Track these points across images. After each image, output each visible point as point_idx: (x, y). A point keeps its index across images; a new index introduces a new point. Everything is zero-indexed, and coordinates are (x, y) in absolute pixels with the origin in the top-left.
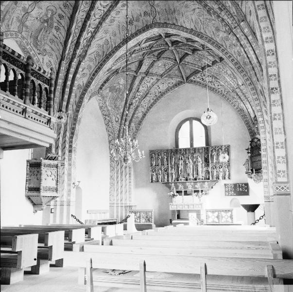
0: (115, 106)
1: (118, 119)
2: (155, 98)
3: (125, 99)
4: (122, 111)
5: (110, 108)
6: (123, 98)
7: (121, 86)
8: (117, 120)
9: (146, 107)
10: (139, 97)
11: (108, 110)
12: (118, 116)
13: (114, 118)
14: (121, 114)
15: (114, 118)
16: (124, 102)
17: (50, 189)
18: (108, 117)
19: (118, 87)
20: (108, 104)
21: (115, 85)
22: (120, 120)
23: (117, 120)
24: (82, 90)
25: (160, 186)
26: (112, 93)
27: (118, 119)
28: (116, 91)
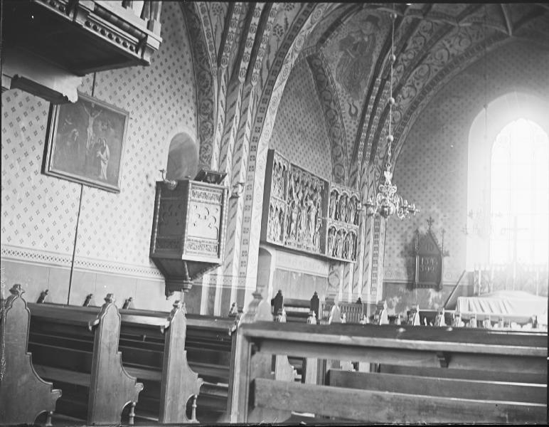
2: (439, 69)
3: (372, 68)
4: (365, 90)
6: (370, 66)
7: (366, 39)
9: (421, 86)
10: (406, 63)
14: (362, 100)
16: (372, 72)
17: (201, 245)
18: (335, 104)
19: (359, 39)
20: (334, 76)
22: (359, 114)
23: (353, 111)
24: (282, 39)
28: (355, 48)
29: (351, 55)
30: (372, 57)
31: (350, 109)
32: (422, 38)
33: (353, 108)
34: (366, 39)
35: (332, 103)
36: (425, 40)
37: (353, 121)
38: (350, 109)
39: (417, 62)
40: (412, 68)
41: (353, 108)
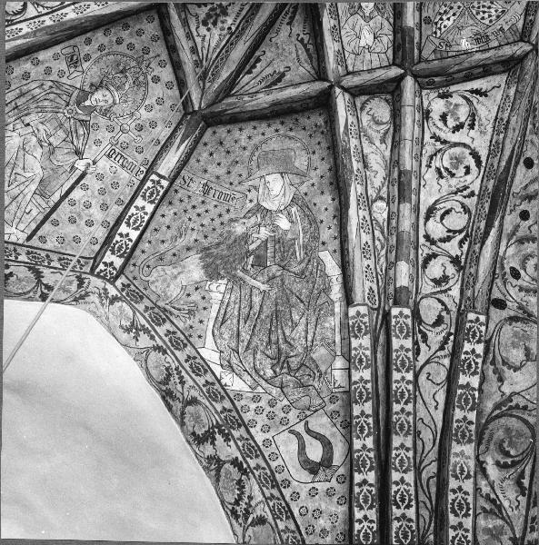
0: (280, 360)
1: (327, 445)
5: (235, 384)
6: (327, 290)
7: (284, 223)
8: (315, 452)
10: (453, 248)
11: (216, 392)
12: (321, 423)
13: (287, 448)
15: (287, 448)
18: (227, 438)
19: (264, 233)
21: (239, 229)
23: (315, 452)
25: (206, 272)
26: (234, 279)
27: (327, 445)
29: (253, 282)
30: (320, 262)
31: (302, 448)
32: (457, 150)
33: (306, 437)
34: (284, 223)
35: (219, 438)
36: (475, 155)
37: (323, 487)
38: (302, 448)
39: (483, 225)
40: (477, 247)
41: (306, 437)
